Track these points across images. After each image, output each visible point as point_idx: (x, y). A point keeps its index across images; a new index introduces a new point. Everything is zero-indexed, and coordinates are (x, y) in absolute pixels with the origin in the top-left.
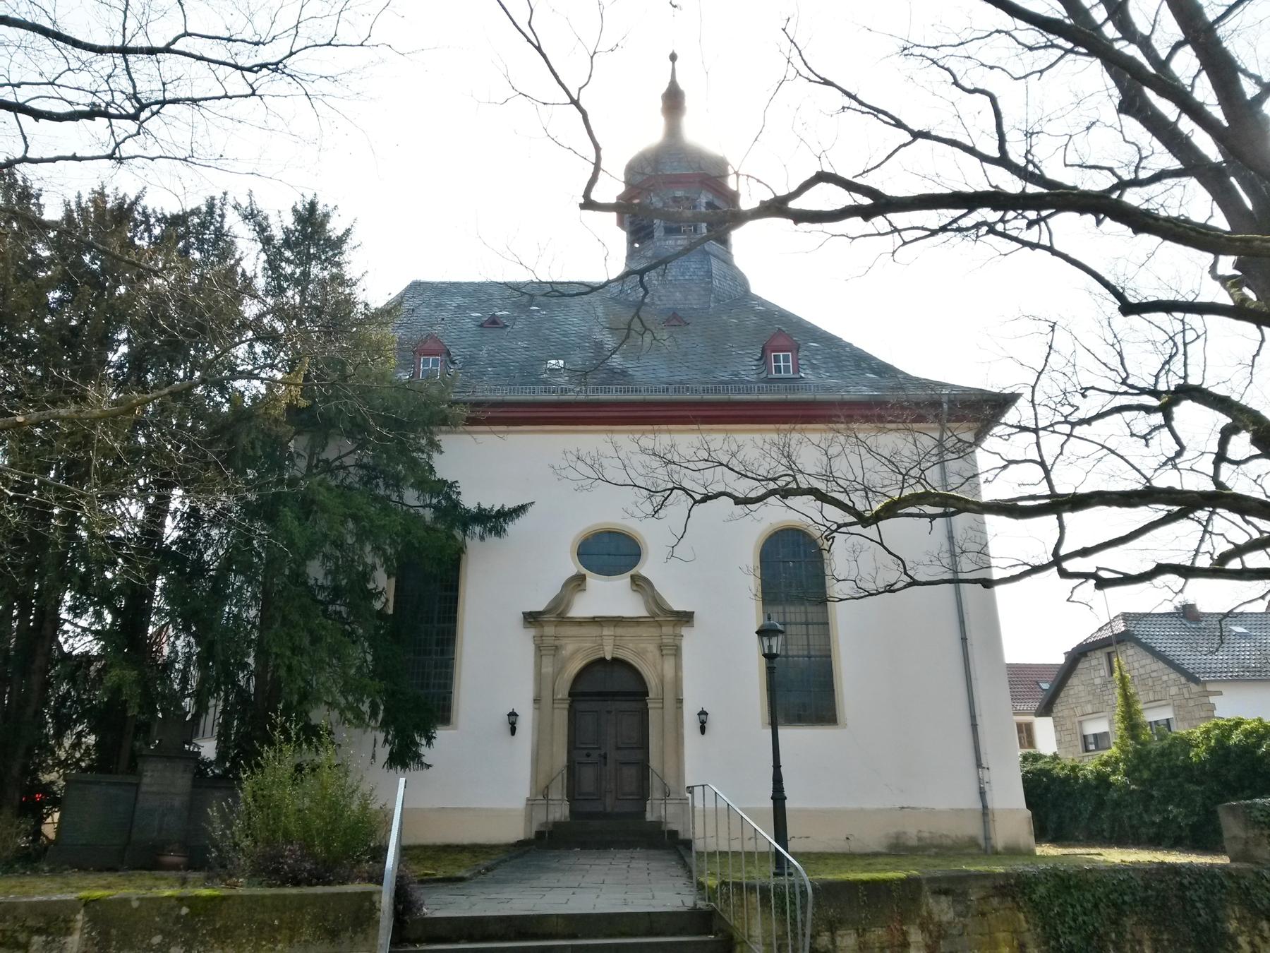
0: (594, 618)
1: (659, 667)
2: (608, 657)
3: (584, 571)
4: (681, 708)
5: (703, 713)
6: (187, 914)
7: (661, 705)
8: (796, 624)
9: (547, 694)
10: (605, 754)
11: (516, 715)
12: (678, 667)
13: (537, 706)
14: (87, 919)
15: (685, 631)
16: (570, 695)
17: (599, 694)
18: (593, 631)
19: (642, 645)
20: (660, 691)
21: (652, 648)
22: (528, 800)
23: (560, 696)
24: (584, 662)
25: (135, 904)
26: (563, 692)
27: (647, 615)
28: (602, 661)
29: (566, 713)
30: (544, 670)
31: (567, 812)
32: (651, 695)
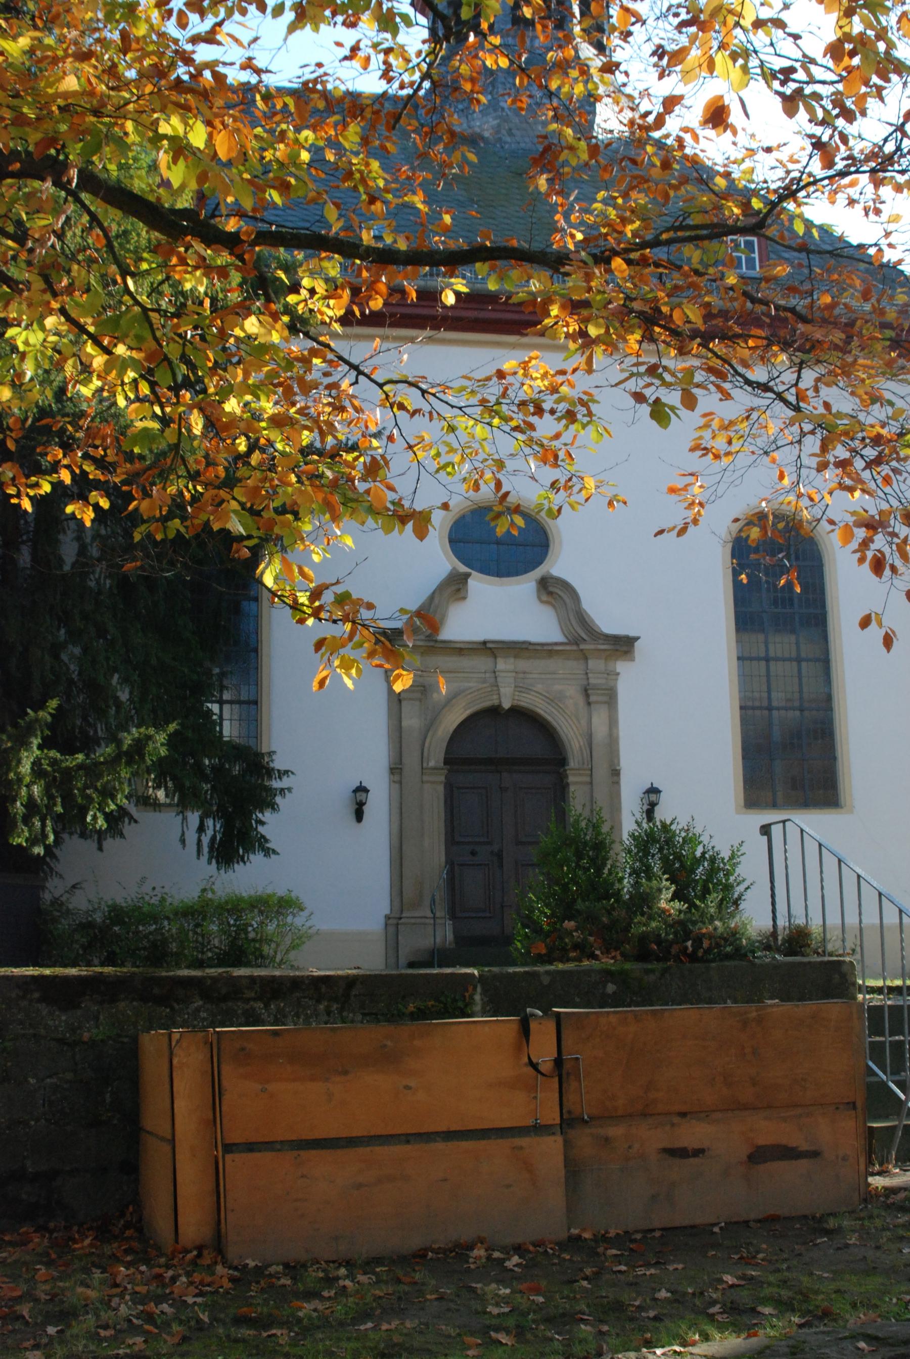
0: (485, 643)
1: (584, 722)
2: (506, 705)
3: (463, 569)
4: (617, 783)
5: (653, 791)
6: (614, 993)
7: (588, 779)
8: (784, 660)
9: (411, 761)
10: (501, 851)
11: (366, 791)
12: (613, 722)
13: (397, 778)
14: (486, 999)
15: (621, 666)
16: (447, 762)
17: (490, 761)
18: (482, 663)
19: (557, 687)
20: (586, 753)
21: (572, 692)
22: (387, 918)
23: (432, 764)
24: (468, 712)
25: (546, 980)
26: (436, 758)
27: (565, 640)
28: (494, 712)
29: (441, 789)
30: (405, 723)
31: (450, 936)
32: (573, 763)
